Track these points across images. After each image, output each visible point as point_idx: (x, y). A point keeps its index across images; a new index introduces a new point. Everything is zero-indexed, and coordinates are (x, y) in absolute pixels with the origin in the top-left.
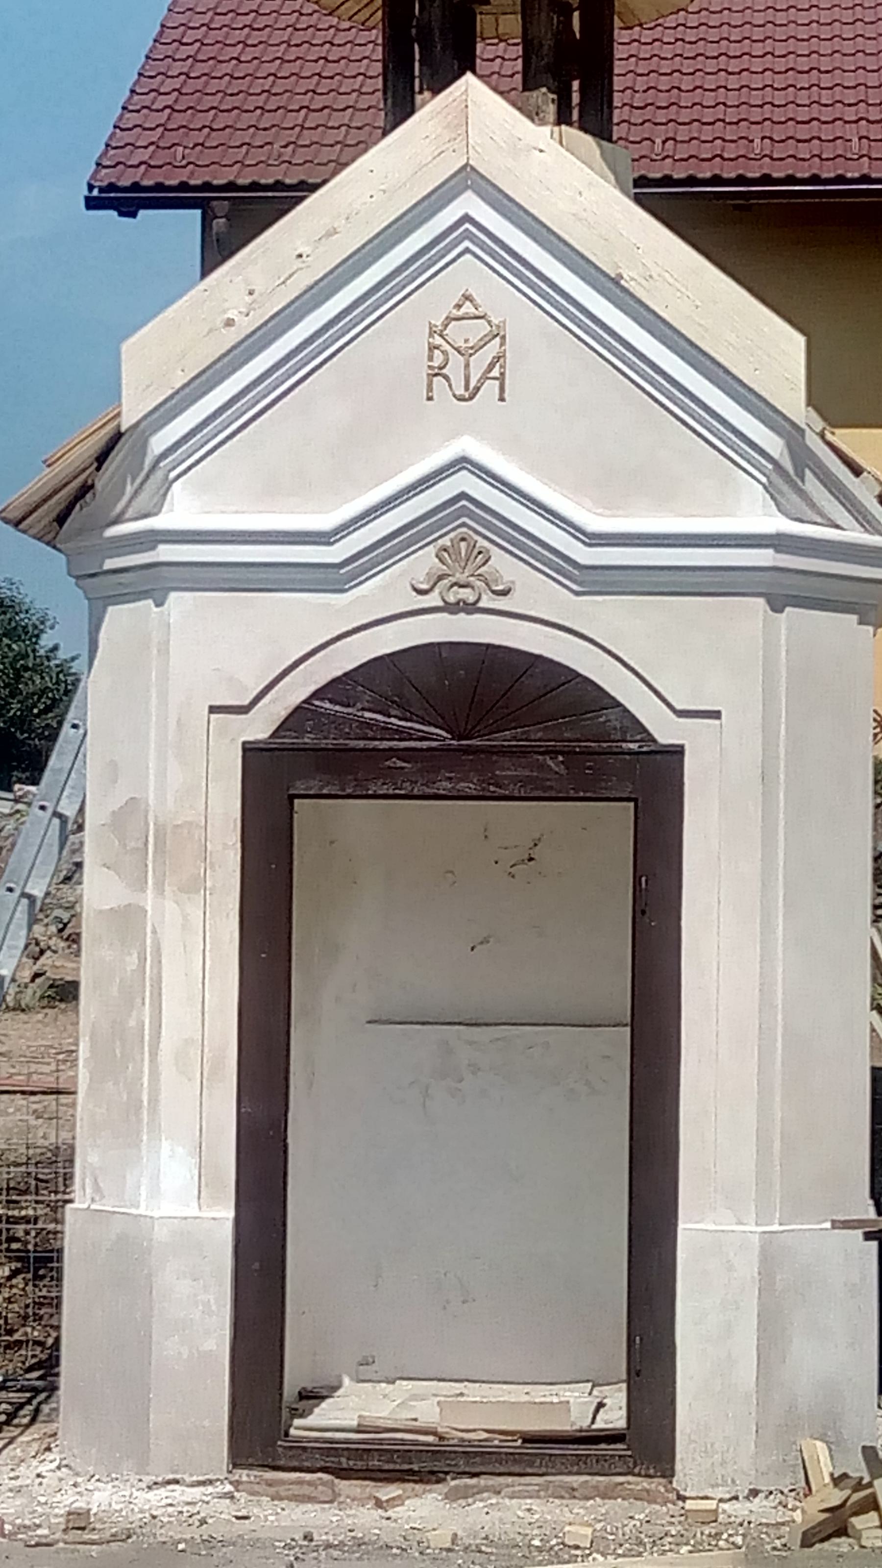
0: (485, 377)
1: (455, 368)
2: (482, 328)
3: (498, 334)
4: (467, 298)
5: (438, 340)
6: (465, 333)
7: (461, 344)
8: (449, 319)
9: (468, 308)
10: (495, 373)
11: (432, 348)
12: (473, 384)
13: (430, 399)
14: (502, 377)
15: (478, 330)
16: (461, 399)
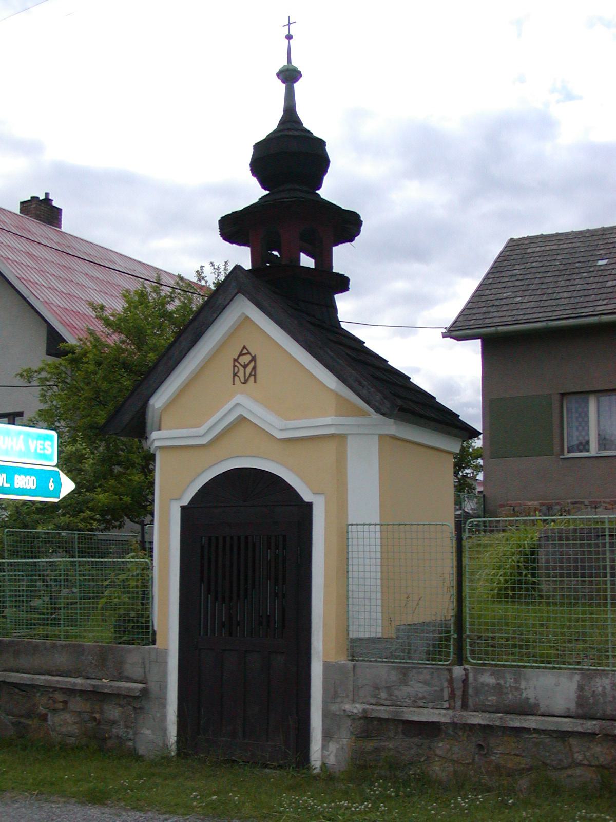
0: (250, 375)
1: (241, 374)
2: (248, 358)
3: (254, 359)
4: (244, 347)
5: (236, 364)
6: (245, 359)
7: (243, 364)
8: (239, 356)
9: (245, 351)
10: (253, 373)
11: (235, 366)
12: (247, 377)
13: (234, 384)
14: (255, 375)
15: (248, 358)
16: (243, 383)
